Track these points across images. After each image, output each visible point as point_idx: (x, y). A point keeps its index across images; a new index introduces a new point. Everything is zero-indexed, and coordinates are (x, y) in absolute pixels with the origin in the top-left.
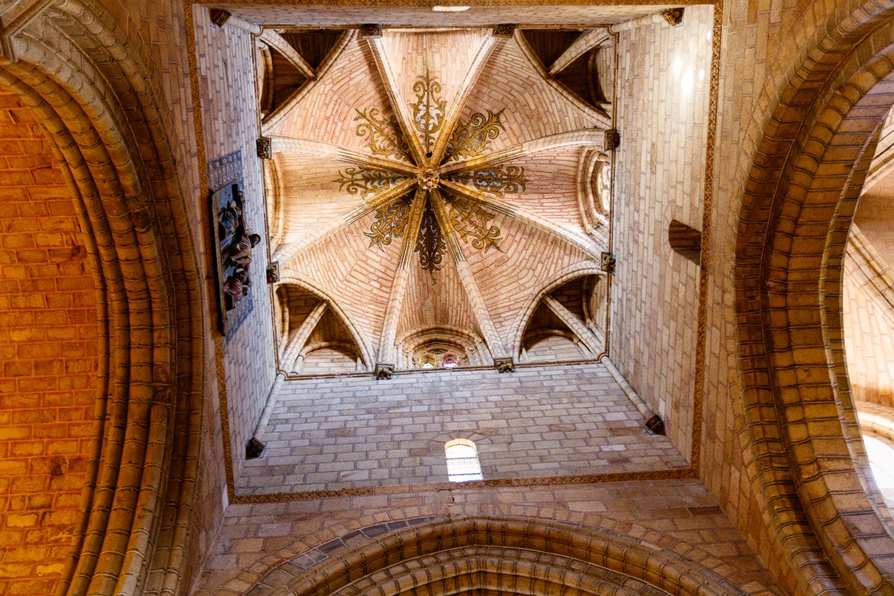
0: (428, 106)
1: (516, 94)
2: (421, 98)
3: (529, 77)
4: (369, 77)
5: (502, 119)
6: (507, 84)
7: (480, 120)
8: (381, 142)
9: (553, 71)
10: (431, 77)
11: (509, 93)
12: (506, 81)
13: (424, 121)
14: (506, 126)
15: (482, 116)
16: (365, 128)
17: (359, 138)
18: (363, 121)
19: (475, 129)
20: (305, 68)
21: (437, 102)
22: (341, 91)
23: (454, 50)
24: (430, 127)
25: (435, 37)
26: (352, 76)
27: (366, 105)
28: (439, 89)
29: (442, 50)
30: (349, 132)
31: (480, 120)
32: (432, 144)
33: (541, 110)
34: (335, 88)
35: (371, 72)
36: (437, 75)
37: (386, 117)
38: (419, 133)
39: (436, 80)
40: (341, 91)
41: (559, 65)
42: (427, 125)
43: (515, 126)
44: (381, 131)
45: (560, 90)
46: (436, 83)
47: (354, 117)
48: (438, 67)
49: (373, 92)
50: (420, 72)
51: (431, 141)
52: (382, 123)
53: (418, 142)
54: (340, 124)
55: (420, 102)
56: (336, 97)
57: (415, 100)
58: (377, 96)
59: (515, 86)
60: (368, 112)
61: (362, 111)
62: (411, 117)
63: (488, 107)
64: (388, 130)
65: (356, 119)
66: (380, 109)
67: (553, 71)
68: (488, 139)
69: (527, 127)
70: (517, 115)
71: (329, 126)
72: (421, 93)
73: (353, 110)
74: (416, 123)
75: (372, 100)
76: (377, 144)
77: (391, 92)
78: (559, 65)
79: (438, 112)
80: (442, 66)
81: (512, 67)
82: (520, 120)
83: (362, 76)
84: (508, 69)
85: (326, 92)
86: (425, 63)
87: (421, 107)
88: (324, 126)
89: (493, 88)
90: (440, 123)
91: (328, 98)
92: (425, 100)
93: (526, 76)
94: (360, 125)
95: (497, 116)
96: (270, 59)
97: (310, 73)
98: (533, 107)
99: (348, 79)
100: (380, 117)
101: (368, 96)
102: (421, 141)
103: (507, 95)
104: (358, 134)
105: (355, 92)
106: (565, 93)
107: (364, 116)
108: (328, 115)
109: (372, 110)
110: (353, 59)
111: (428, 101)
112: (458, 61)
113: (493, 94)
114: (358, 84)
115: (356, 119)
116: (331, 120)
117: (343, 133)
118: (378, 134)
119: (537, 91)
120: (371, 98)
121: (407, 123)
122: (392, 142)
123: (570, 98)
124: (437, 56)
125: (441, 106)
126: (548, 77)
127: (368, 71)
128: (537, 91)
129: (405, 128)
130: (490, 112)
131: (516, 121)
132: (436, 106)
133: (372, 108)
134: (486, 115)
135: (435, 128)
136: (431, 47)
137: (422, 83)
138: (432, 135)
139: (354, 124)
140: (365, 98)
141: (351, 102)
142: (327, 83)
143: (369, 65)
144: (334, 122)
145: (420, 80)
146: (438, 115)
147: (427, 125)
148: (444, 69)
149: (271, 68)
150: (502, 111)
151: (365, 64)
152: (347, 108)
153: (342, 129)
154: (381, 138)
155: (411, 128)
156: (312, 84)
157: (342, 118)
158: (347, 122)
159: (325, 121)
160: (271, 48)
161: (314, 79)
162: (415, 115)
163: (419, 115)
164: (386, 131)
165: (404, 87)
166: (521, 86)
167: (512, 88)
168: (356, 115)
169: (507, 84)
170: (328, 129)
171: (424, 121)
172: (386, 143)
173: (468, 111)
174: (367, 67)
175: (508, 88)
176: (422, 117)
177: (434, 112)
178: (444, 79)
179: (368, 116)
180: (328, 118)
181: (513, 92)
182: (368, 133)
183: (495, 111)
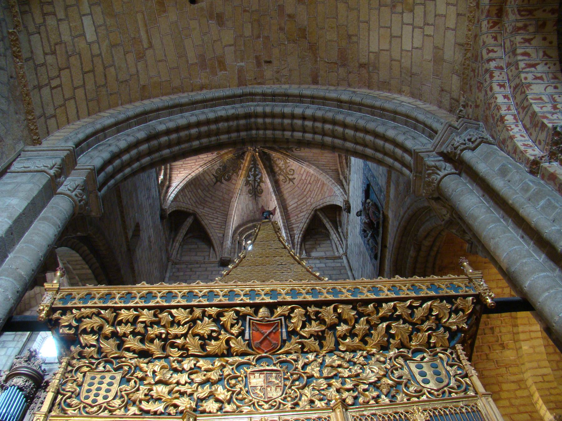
0: (255, 180)
1: (208, 195)
2: (259, 185)
3: (203, 209)
4: (287, 202)
5: (214, 180)
6: (214, 201)
7: (226, 177)
8: (281, 163)
9: (192, 217)
10: (254, 196)
11: (212, 196)
12: (215, 203)
13: (257, 173)
14: (212, 177)
15: (226, 180)
16: (290, 173)
17: (293, 168)
18: (290, 177)
19: (229, 172)
20: (321, 216)
21: (250, 184)
22: (302, 196)
23: (243, 214)
24: (253, 170)
25: (252, 218)
26: (296, 205)
27: (288, 186)
28: (249, 192)
29: (249, 212)
30: (298, 173)
31: (226, 177)
32: (252, 161)
33: (195, 191)
34: (305, 199)
35: (286, 205)
36: (251, 199)
37: (278, 177)
38: (259, 166)
39: (250, 195)
40: (302, 196)
41: (190, 220)
42: (255, 171)
43: (208, 178)
44: (280, 169)
45: (188, 210)
46: (251, 194)
47: (295, 180)
48: (250, 203)
49: (285, 192)
50: (260, 199)
51: (252, 163)
52: (280, 174)
53: (261, 165)
54: (303, 178)
55: (259, 183)
56: (305, 193)
57: (262, 184)
58: (282, 190)
59: (210, 200)
60: (288, 182)
61: (291, 182)
62: (264, 176)
63: (223, 186)
64: (277, 169)
65: (294, 179)
66: (281, 183)
67: (192, 217)
68: (221, 168)
69: (201, 179)
70: (207, 184)
71: (309, 179)
72: (259, 188)
73: (296, 184)
74: (261, 173)
75: (286, 187)
76: (282, 162)
77: (276, 195)
78: (190, 220)
79: (249, 179)
80: (248, 204)
81: (213, 213)
82: (205, 181)
83: (292, 204)
84: (215, 212)
85: (310, 198)
86: (257, 204)
87: (259, 181)
88: (312, 180)
89: (221, 197)
90: (248, 173)
91: (309, 194)
92: (257, 184)
93: (206, 209)
94: (292, 175)
95: (217, 181)
96: (338, 219)
97: (318, 213)
98: (199, 191)
99: (299, 203)
100: (281, 178)
101: (287, 191)
102: (258, 162)
103: (213, 194)
104: (294, 170)
105: (295, 194)
106: (185, 210)
107: (291, 180)
108: (309, 185)
109: (285, 182)
110: (296, 217)
111: (255, 183)
112: (240, 209)
113: (221, 194)
114: (293, 198)
115: (294, 179)
116: (308, 182)
117: (302, 172)
118: (282, 168)
119: (198, 201)
120: (286, 188)
121: (267, 175)
122: (275, 162)
123: (182, 209)
124: (251, 208)
125: (247, 183)
126: (194, 215)
127: (288, 206)
128: (198, 201)
129: (268, 173)
130: (222, 183)
131: (207, 181)
132: (250, 182)
133: (286, 184)
134: (223, 181)
135: (250, 170)
136: (255, 212)
137: (258, 193)
138: (252, 166)
139: (296, 176)
140: (289, 190)
141: (297, 189)
142: (309, 203)
143: (287, 211)
144: (307, 180)
145: (259, 195)
146: (249, 177)
147: (255, 171)
148: (247, 203)
149: (337, 214)
150: (215, 184)
151: (289, 212)
152: (299, 186)
153: (302, 176)
154: (281, 165)
155: (264, 172)
156: (318, 207)
157: (302, 181)
158: (300, 178)
159: (311, 182)
160: (337, 229)
161: (316, 210)
162: (262, 177)
163: (260, 176)
164: (278, 169)
165: (268, 194)
166: (207, 201)
167: (211, 198)
168: (295, 181)
169: (214, 201)
170: (310, 178)
171: (257, 173)
172: (278, 162)
173: (234, 182)
174: (289, 209)
175: (213, 198)
176: (258, 175)
177: (252, 178)
178: (247, 197)
179: (288, 179)
180: (309, 183)
181: (210, 196)
182: (288, 169)
183: (219, 183)
